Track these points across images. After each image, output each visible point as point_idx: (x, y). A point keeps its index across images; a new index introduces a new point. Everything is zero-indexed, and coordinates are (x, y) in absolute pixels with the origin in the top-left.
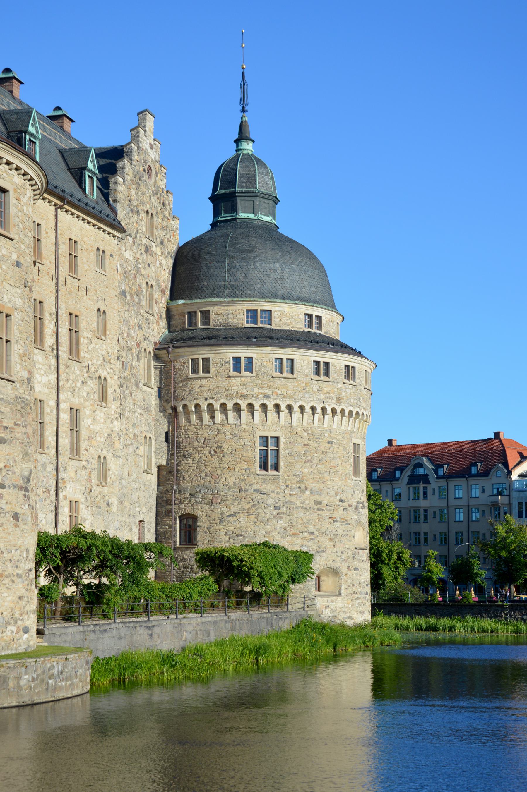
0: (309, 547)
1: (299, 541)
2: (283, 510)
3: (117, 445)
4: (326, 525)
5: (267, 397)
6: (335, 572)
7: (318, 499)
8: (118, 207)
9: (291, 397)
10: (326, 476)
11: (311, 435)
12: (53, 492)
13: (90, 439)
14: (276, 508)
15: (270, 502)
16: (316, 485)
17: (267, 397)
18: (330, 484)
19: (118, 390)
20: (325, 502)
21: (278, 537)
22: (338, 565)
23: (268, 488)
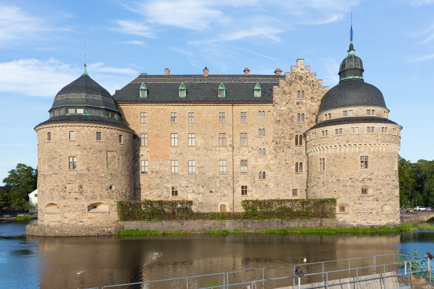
0: (335, 196)
1: (330, 194)
2: (325, 184)
3: (272, 167)
4: (341, 188)
5: (319, 145)
6: (347, 205)
7: (338, 179)
8: (274, 96)
9: (327, 144)
10: (342, 170)
11: (336, 156)
12: (231, 184)
13: (254, 167)
14: (323, 183)
16: (338, 174)
17: (319, 145)
18: (345, 173)
19: (273, 151)
20: (341, 180)
21: (323, 193)
22: (347, 203)
23: (321, 176)
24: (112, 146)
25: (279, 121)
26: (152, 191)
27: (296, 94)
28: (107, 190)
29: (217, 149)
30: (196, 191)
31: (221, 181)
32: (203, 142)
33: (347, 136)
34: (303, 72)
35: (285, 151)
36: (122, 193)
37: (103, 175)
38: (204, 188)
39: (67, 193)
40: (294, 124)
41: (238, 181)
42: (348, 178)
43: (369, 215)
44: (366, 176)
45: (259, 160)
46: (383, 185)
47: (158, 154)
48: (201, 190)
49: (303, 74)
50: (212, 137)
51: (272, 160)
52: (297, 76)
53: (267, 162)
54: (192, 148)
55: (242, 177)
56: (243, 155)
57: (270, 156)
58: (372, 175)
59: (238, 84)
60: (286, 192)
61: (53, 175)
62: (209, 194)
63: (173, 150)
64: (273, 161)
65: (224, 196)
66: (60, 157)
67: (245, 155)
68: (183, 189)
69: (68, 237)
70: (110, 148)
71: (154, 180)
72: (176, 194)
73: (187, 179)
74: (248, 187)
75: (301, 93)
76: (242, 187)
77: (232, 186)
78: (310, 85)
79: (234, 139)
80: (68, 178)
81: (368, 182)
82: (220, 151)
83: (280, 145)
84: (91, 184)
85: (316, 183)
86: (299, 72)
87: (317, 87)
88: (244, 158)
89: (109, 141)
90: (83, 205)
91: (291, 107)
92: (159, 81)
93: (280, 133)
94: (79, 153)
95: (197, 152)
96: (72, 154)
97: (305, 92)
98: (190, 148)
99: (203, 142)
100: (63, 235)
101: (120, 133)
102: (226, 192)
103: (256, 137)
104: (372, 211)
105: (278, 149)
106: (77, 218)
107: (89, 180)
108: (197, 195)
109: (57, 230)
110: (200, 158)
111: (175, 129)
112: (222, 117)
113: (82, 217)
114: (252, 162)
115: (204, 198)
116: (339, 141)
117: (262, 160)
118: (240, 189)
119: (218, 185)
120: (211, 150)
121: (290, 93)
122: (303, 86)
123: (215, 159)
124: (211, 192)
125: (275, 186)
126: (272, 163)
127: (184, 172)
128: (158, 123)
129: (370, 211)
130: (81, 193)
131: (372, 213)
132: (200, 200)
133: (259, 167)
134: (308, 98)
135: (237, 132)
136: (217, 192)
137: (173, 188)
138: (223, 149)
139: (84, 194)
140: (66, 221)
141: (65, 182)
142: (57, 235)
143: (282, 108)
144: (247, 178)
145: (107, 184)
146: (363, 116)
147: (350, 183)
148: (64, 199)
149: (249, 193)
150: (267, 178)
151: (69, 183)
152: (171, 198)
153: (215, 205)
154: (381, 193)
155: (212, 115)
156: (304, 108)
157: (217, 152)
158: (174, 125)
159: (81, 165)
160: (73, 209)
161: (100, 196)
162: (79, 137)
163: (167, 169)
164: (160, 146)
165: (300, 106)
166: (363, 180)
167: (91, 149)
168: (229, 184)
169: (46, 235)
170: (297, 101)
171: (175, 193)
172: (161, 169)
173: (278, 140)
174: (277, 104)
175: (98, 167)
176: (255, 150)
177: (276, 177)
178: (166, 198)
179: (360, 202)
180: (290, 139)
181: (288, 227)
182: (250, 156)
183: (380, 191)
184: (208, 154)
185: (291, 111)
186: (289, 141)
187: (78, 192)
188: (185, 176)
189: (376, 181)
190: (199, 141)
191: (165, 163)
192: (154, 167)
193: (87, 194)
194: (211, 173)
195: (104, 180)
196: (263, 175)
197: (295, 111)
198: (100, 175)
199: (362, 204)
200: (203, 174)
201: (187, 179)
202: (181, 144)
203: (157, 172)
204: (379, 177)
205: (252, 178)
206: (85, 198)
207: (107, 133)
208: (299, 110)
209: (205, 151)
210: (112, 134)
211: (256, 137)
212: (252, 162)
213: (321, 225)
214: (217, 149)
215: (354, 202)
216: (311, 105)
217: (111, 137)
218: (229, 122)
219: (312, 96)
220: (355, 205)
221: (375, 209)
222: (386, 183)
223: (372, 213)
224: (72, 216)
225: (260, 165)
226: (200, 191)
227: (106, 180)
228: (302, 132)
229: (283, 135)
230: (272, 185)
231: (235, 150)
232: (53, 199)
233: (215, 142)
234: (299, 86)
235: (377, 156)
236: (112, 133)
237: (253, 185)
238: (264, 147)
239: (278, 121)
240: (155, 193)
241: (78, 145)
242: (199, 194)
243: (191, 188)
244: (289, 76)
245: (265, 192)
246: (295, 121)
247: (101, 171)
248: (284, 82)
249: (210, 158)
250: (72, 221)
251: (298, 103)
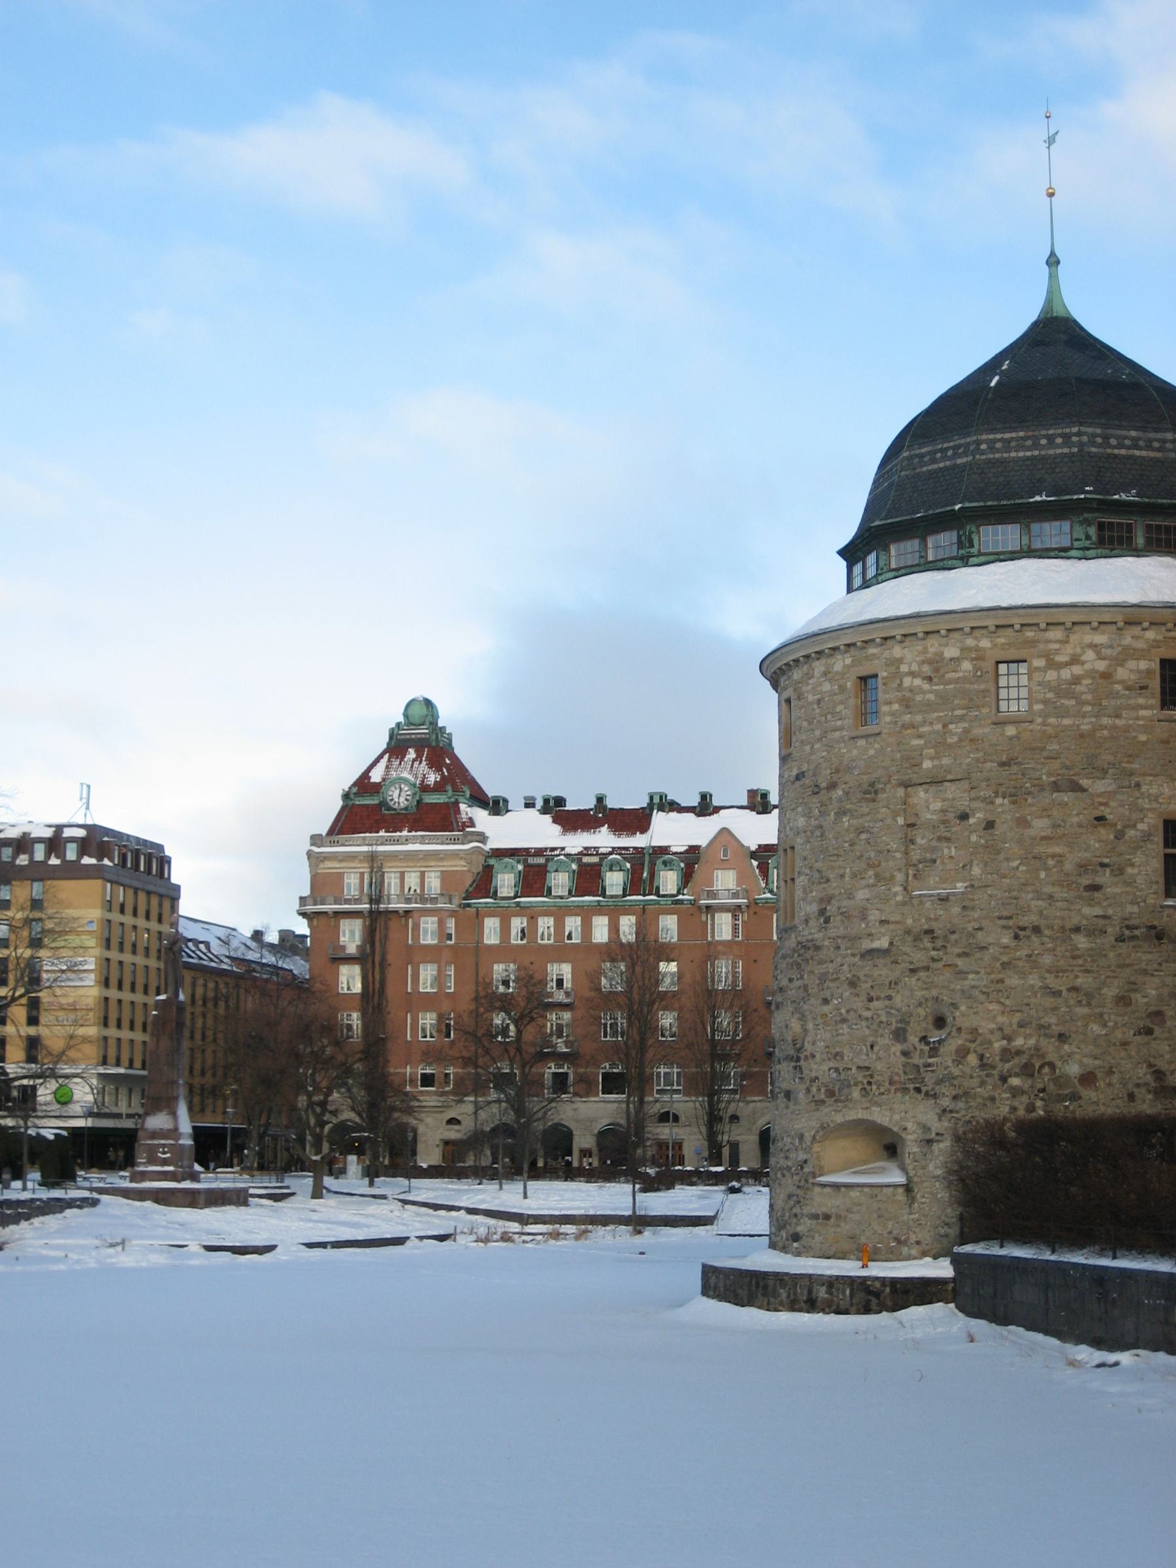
24: (940, 745)
28: (899, 1035)
36: (1007, 1055)
37: (883, 943)
70: (927, 764)
89: (919, 718)
145: (898, 1000)
175: (862, 894)
195: (884, 971)
198: (867, 944)
207: (904, 668)
227: (893, 976)
247: (874, 916)
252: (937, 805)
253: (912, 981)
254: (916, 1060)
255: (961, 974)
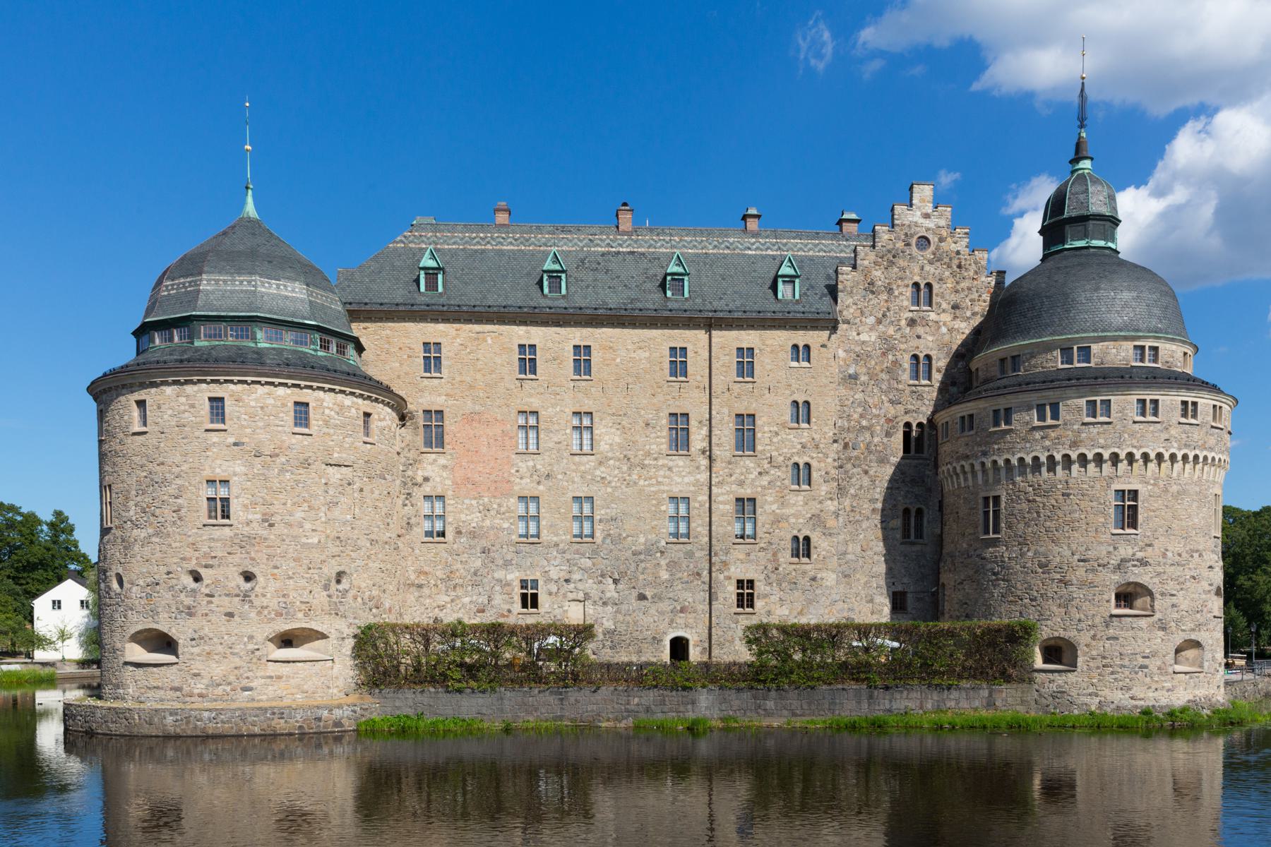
3: (831, 523)
9: (1008, 450)
12: (705, 573)
15: (989, 566)
19: (834, 472)
25: (854, 377)
26: (460, 592)
27: (909, 292)
28: (326, 587)
29: (661, 462)
30: (595, 594)
31: (672, 565)
32: (617, 439)
33: (1076, 427)
34: (929, 224)
35: (871, 473)
38: (620, 587)
39: (200, 598)
40: (900, 387)
41: (725, 563)
42: (1076, 557)
43: (1136, 673)
44: (1130, 552)
45: (792, 498)
46: (1181, 580)
47: (476, 477)
48: (610, 590)
49: (928, 230)
50: (647, 425)
51: (831, 499)
52: (912, 236)
53: (815, 507)
54: (585, 458)
55: (739, 553)
56: (741, 484)
57: (824, 489)
58: (1149, 549)
59: (725, 256)
60: (871, 601)
61: (154, 539)
62: (636, 604)
63: (525, 465)
64: (836, 503)
65: (682, 611)
66: (178, 481)
67: (748, 482)
68: (554, 588)
69: (208, 737)
70: (336, 455)
71: (464, 557)
72: (535, 604)
73: (567, 556)
74: (757, 584)
75: (923, 293)
76: (740, 583)
77: (707, 579)
78: (949, 266)
79: (715, 432)
80: (206, 549)
81: (1136, 570)
82: (670, 469)
83: (855, 453)
84: (276, 567)
85: (971, 573)
86: (916, 224)
87: (971, 273)
88: (746, 492)
89: (332, 431)
90: (251, 638)
91: (891, 331)
92: (478, 243)
93: (856, 416)
94: (240, 469)
95: (598, 473)
96: (218, 470)
97: (936, 286)
98: (577, 458)
99: (617, 439)
100: (189, 733)
101: (366, 406)
102: (687, 597)
103: (784, 425)
104: (1146, 662)
105: (849, 466)
106: (232, 678)
107: (270, 557)
108: (600, 609)
109: (171, 714)
110: (609, 490)
111: (531, 395)
112: (678, 364)
113: (250, 674)
114: (768, 507)
115: (620, 617)
116: (1047, 443)
117: (801, 498)
118: (732, 589)
119: (665, 575)
120: (643, 467)
121: (890, 291)
122: (927, 268)
123: (655, 493)
124: (642, 597)
125: (838, 582)
126: (832, 508)
127: (557, 535)
128: (479, 376)
129: (1141, 661)
130: (245, 596)
131: (1146, 667)
132: (609, 624)
133: (792, 520)
134: (944, 306)
135: (726, 410)
136: (658, 598)
137: (524, 583)
138: (681, 463)
139: (257, 602)
140: (199, 687)
141: (194, 562)
142: (171, 730)
143: (864, 337)
144: (752, 557)
145: (325, 570)
146: (1122, 364)
147: (1081, 572)
148: (191, 615)
149: (759, 604)
150: (814, 556)
151: (206, 567)
152: (517, 616)
153: (654, 638)
154: (1173, 606)
155: (647, 354)
156: (930, 338)
157: (662, 473)
158: (527, 385)
159: (245, 506)
160: (220, 648)
161: (303, 607)
162: (238, 418)
163: (506, 525)
164: (484, 450)
165: (920, 330)
166: (1119, 567)
167: (277, 455)
168: (698, 574)
169: (135, 731)
170: (911, 315)
171: (530, 601)
172: (487, 523)
173: (850, 437)
174: (848, 323)
175: (299, 515)
176: (779, 467)
177: (845, 553)
178: (503, 616)
179: (1111, 632)
180: (888, 434)
181: (889, 711)
182: (764, 488)
183: (1174, 600)
184: (635, 477)
185: (888, 346)
186: (885, 440)
187: (237, 595)
188: (561, 546)
189: (1160, 569)
190: (607, 438)
191: (500, 505)
192: (463, 517)
193: (265, 602)
194: (642, 540)
196: (803, 547)
197: (903, 346)
198: (304, 540)
199: (1117, 639)
200: (617, 540)
201: (567, 556)
202: (551, 445)
203: (473, 535)
204: (1169, 554)
205: (769, 556)
206: (259, 613)
208: (915, 342)
209: (625, 468)
210: (341, 409)
211: (784, 425)
212: (773, 503)
213: (990, 704)
214: (661, 462)
215: (1092, 632)
216: (950, 330)
217: (337, 420)
218: (699, 378)
219: (954, 298)
220: (1094, 643)
221: (1154, 654)
222: (1188, 574)
223: (1146, 667)
224: (217, 670)
225: (796, 516)
226: (608, 595)
227: (323, 557)
228: (924, 414)
229: (864, 423)
230: (830, 578)
231: (717, 466)
232: (154, 613)
233: (660, 440)
234: (917, 270)
235: (1166, 491)
236: (342, 407)
237: (773, 577)
238: (807, 459)
239: (850, 376)
240: (466, 600)
241: (235, 444)
242: (604, 603)
243: (580, 585)
244: (886, 237)
245: (810, 602)
246: (905, 376)
247: (308, 526)
248: (872, 256)
249: (641, 491)
250: (219, 685)
251: (912, 323)
252: (339, 476)
253: (333, 562)
254: (334, 599)
255: (353, 560)
